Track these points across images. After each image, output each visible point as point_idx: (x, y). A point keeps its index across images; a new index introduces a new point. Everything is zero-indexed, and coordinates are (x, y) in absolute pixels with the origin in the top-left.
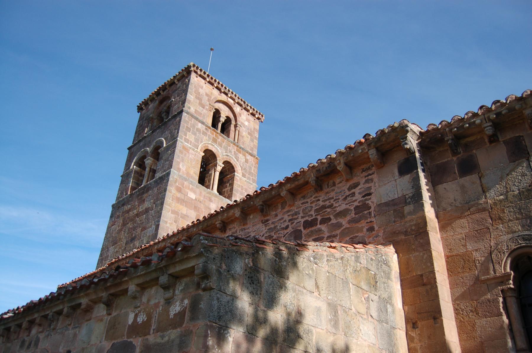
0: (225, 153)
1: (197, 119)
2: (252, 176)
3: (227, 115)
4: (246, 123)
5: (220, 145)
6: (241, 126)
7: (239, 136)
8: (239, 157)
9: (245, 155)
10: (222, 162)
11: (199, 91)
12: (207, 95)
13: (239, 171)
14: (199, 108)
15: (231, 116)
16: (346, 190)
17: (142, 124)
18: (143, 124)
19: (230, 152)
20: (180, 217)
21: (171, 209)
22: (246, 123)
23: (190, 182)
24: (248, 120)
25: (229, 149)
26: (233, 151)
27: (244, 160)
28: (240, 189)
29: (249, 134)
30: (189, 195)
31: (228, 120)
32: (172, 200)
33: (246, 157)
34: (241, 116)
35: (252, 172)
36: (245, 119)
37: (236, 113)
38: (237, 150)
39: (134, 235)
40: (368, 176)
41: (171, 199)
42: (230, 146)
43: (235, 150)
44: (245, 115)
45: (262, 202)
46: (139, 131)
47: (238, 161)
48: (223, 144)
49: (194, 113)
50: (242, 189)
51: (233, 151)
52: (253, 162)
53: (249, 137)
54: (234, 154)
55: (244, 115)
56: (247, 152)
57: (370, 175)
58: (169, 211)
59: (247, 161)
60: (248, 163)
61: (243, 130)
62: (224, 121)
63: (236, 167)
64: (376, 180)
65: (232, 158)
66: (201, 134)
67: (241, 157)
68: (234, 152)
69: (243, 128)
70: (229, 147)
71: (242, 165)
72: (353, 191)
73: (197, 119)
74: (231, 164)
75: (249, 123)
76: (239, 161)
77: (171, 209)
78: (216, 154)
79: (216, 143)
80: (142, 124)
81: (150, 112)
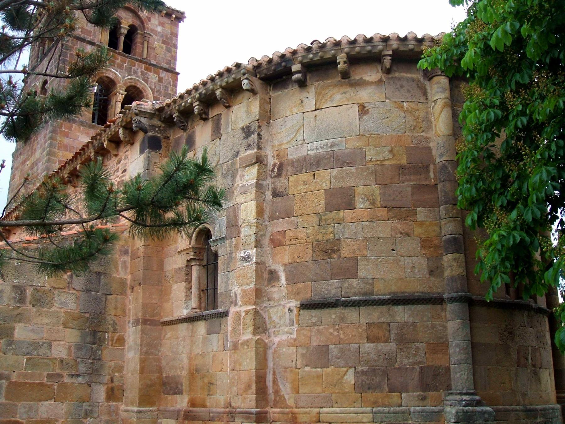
0: (129, 75)
1: (83, 40)
3: (131, 23)
4: (159, 29)
5: (120, 67)
6: (150, 35)
7: (149, 49)
8: (149, 77)
9: (155, 73)
10: (124, 89)
15: (137, 23)
16: (115, 165)
19: (135, 73)
22: (159, 29)
23: (80, 123)
24: (162, 24)
25: (134, 70)
26: (139, 71)
27: (157, 79)
29: (164, 42)
30: (80, 139)
31: (133, 30)
33: (159, 75)
34: (150, 21)
35: (169, 92)
36: (157, 24)
37: (143, 18)
38: (146, 69)
40: (125, 152)
41: (57, 148)
42: (134, 66)
43: (143, 70)
44: (157, 18)
45: (68, 174)
46: (32, 56)
47: (147, 82)
48: (125, 65)
49: (80, 33)
51: (139, 71)
52: (170, 79)
53: (164, 46)
54: (142, 74)
55: (155, 18)
56: (161, 68)
57: (127, 151)
58: (55, 163)
59: (160, 80)
60: (162, 82)
61: (154, 39)
62: (126, 32)
63: (145, 91)
64: (129, 157)
65: (138, 81)
67: (151, 77)
68: (142, 72)
69: (154, 36)
70: (133, 68)
71: (153, 87)
72: (118, 165)
73: (83, 40)
74: (138, 88)
75: (163, 27)
76: (149, 82)
77: (57, 159)
78: (116, 80)
79: (115, 67)
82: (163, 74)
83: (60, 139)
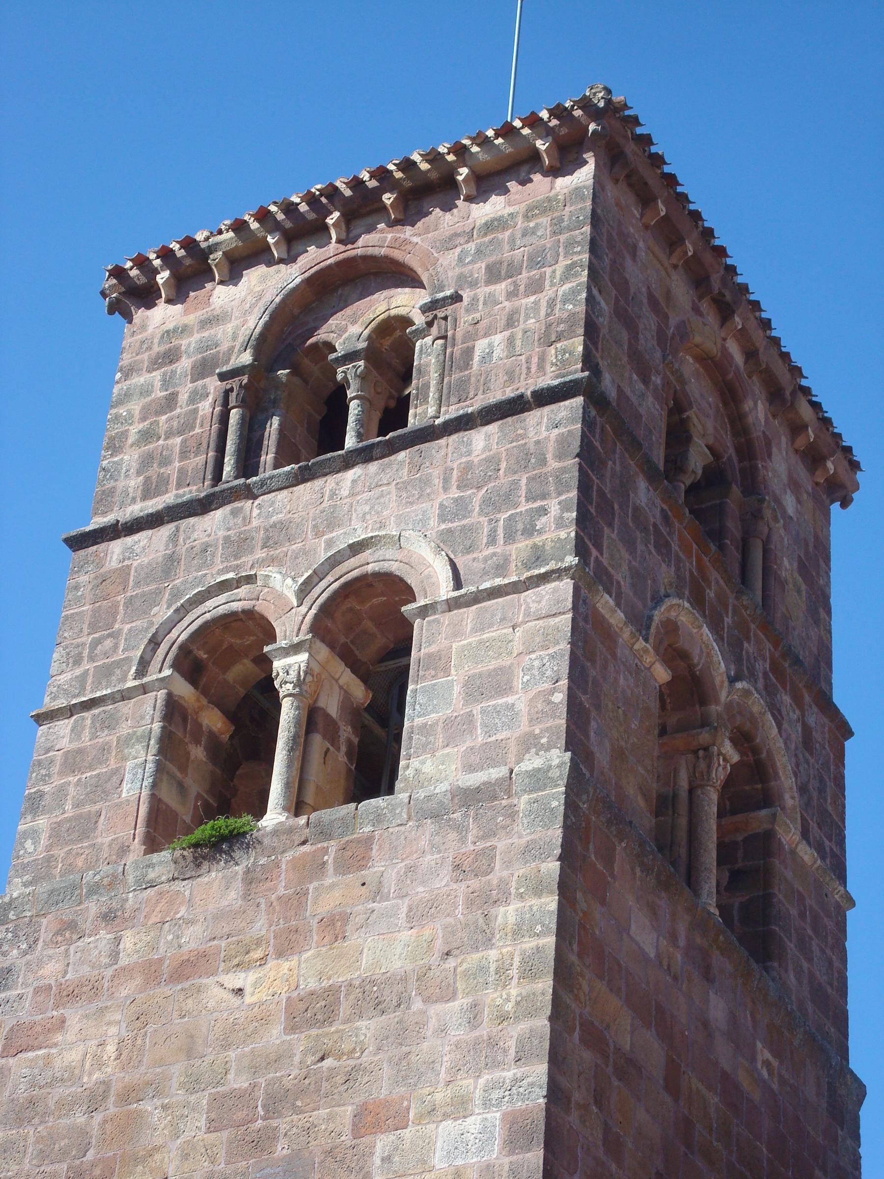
2: (830, 840)
11: (627, 276)
12: (653, 302)
13: (789, 802)
14: (631, 378)
17: (171, 401)
18: (183, 397)
20: (610, 1070)
21: (578, 1012)
28: (794, 912)
32: (580, 956)
39: (281, 1149)
50: (802, 915)
54: (766, 687)
66: (652, 548)
77: (578, 1012)
80: (171, 401)
81: (229, 327)
82: (814, 717)
83: (584, 905)
